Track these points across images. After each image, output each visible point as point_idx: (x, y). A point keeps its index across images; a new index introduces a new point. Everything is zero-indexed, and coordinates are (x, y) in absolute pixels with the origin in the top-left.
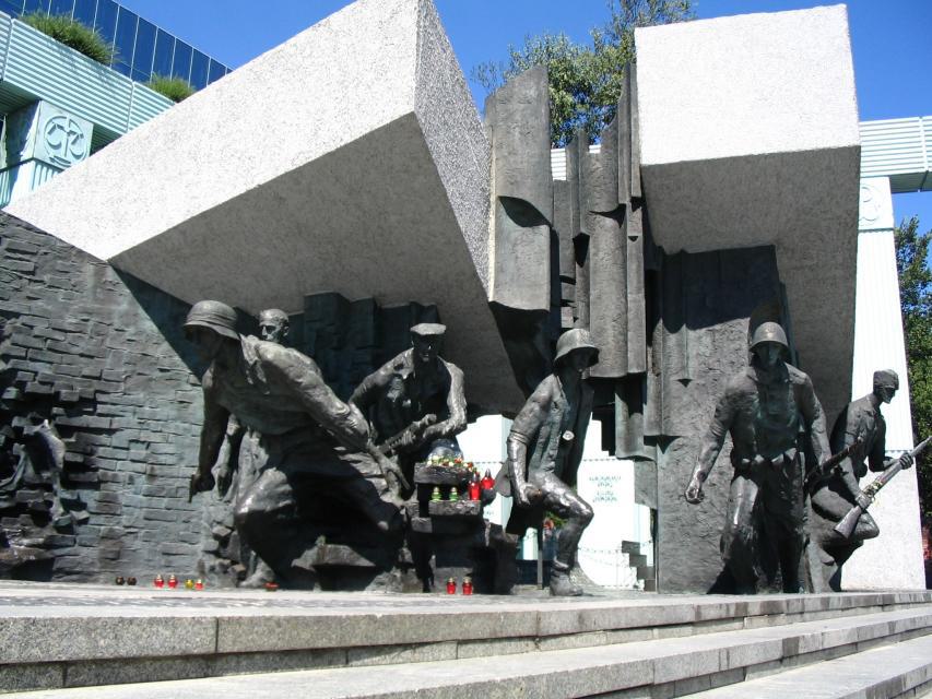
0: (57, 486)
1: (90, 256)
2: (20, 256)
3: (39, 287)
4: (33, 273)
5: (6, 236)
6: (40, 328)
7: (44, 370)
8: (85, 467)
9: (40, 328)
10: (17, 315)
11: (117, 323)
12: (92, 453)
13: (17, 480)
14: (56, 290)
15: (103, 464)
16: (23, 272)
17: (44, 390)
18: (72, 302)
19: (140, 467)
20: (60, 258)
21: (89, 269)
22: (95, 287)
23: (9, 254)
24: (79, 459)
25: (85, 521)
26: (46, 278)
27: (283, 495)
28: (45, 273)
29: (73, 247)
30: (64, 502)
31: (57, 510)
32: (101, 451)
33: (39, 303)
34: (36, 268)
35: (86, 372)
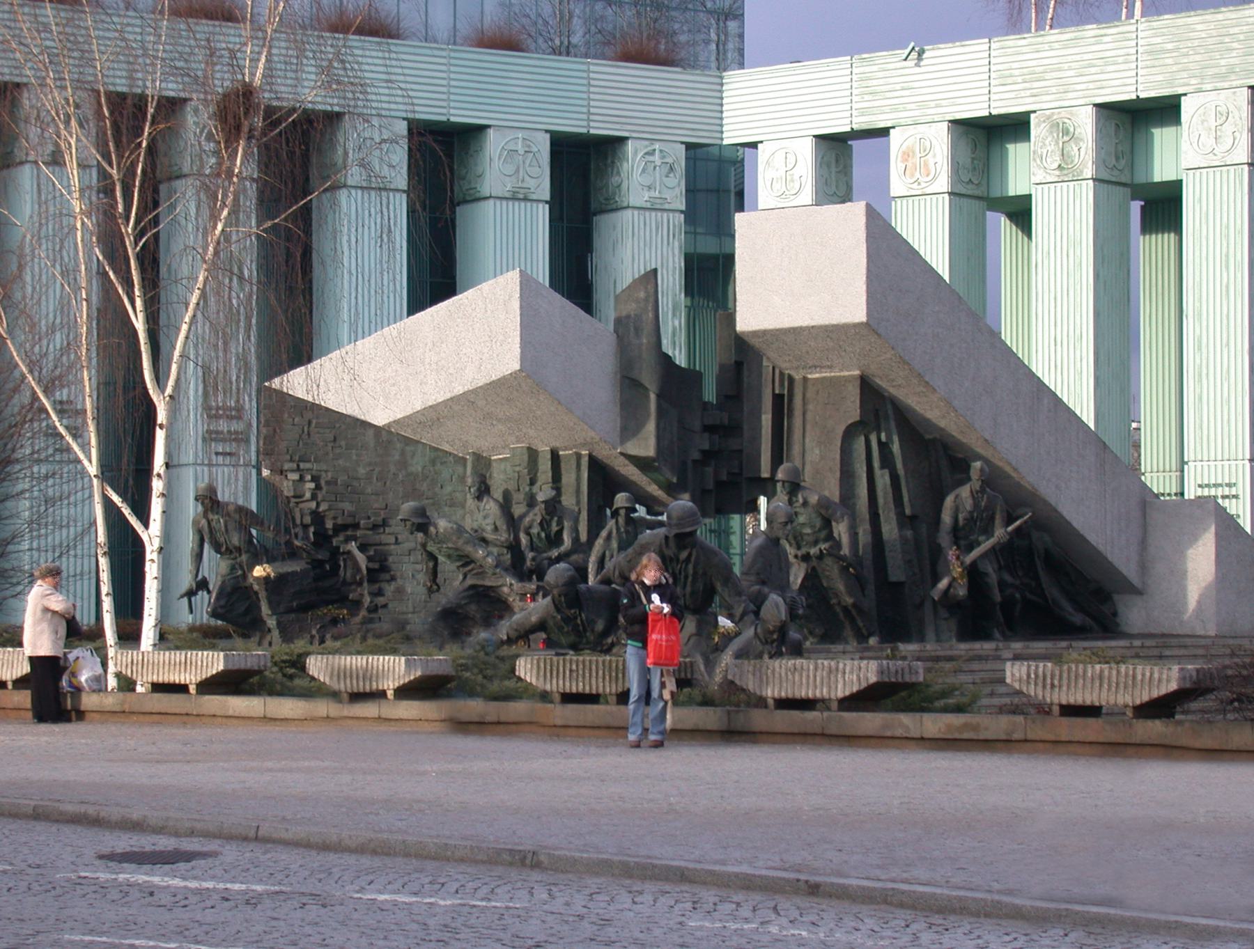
0: (365, 584)
3: (337, 451)
6: (342, 479)
7: (347, 506)
8: (384, 568)
9: (342, 479)
10: (326, 471)
11: (393, 469)
12: (386, 560)
15: (394, 566)
17: (349, 521)
19: (419, 567)
21: (371, 432)
24: (376, 566)
25: (385, 606)
27: (464, 598)
30: (370, 594)
31: (367, 600)
32: (391, 559)
33: (341, 462)
35: (376, 506)
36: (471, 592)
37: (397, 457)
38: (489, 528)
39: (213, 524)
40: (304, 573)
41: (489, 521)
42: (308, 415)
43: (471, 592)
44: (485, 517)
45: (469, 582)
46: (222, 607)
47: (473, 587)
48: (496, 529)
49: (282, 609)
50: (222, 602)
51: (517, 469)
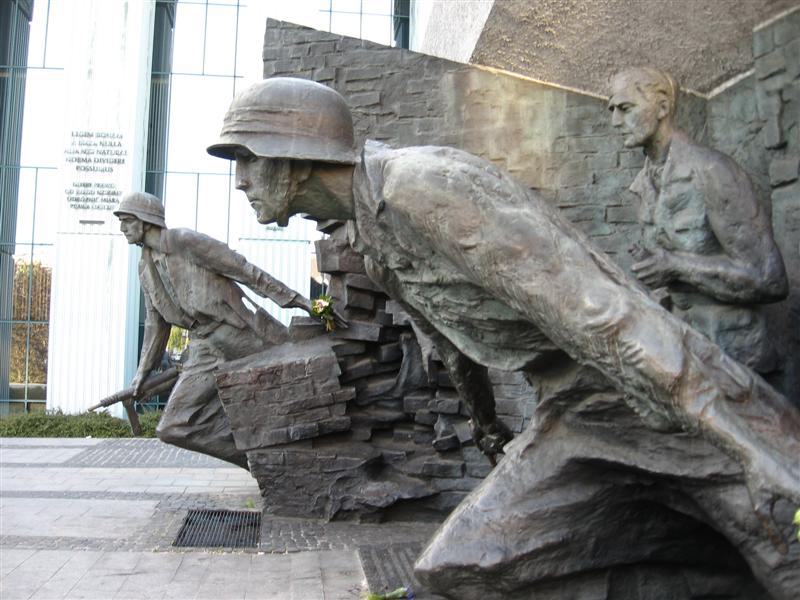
1: (446, 62)
2: (361, 86)
3: (388, 122)
4: (379, 104)
5: (344, 66)
13: (403, 380)
14: (410, 119)
16: (367, 107)
18: (431, 133)
20: (410, 76)
21: (448, 78)
22: (458, 104)
23: (350, 87)
26: (396, 107)
28: (394, 101)
29: (425, 56)
34: (382, 97)
36: (577, 495)
37: (500, 124)
38: (688, 241)
39: (160, 269)
40: (320, 369)
41: (691, 216)
42: (338, 60)
43: (577, 495)
44: (674, 207)
45: (572, 446)
46: (181, 425)
47: (582, 470)
48: (713, 245)
49: (264, 437)
50: (185, 417)
51: (777, 83)
